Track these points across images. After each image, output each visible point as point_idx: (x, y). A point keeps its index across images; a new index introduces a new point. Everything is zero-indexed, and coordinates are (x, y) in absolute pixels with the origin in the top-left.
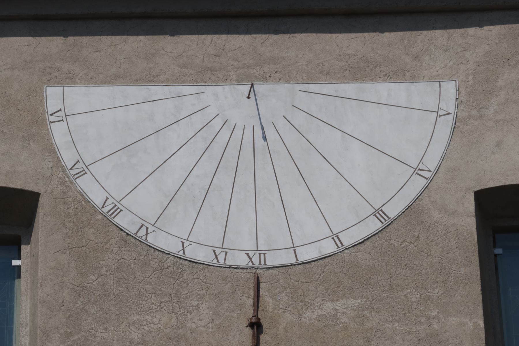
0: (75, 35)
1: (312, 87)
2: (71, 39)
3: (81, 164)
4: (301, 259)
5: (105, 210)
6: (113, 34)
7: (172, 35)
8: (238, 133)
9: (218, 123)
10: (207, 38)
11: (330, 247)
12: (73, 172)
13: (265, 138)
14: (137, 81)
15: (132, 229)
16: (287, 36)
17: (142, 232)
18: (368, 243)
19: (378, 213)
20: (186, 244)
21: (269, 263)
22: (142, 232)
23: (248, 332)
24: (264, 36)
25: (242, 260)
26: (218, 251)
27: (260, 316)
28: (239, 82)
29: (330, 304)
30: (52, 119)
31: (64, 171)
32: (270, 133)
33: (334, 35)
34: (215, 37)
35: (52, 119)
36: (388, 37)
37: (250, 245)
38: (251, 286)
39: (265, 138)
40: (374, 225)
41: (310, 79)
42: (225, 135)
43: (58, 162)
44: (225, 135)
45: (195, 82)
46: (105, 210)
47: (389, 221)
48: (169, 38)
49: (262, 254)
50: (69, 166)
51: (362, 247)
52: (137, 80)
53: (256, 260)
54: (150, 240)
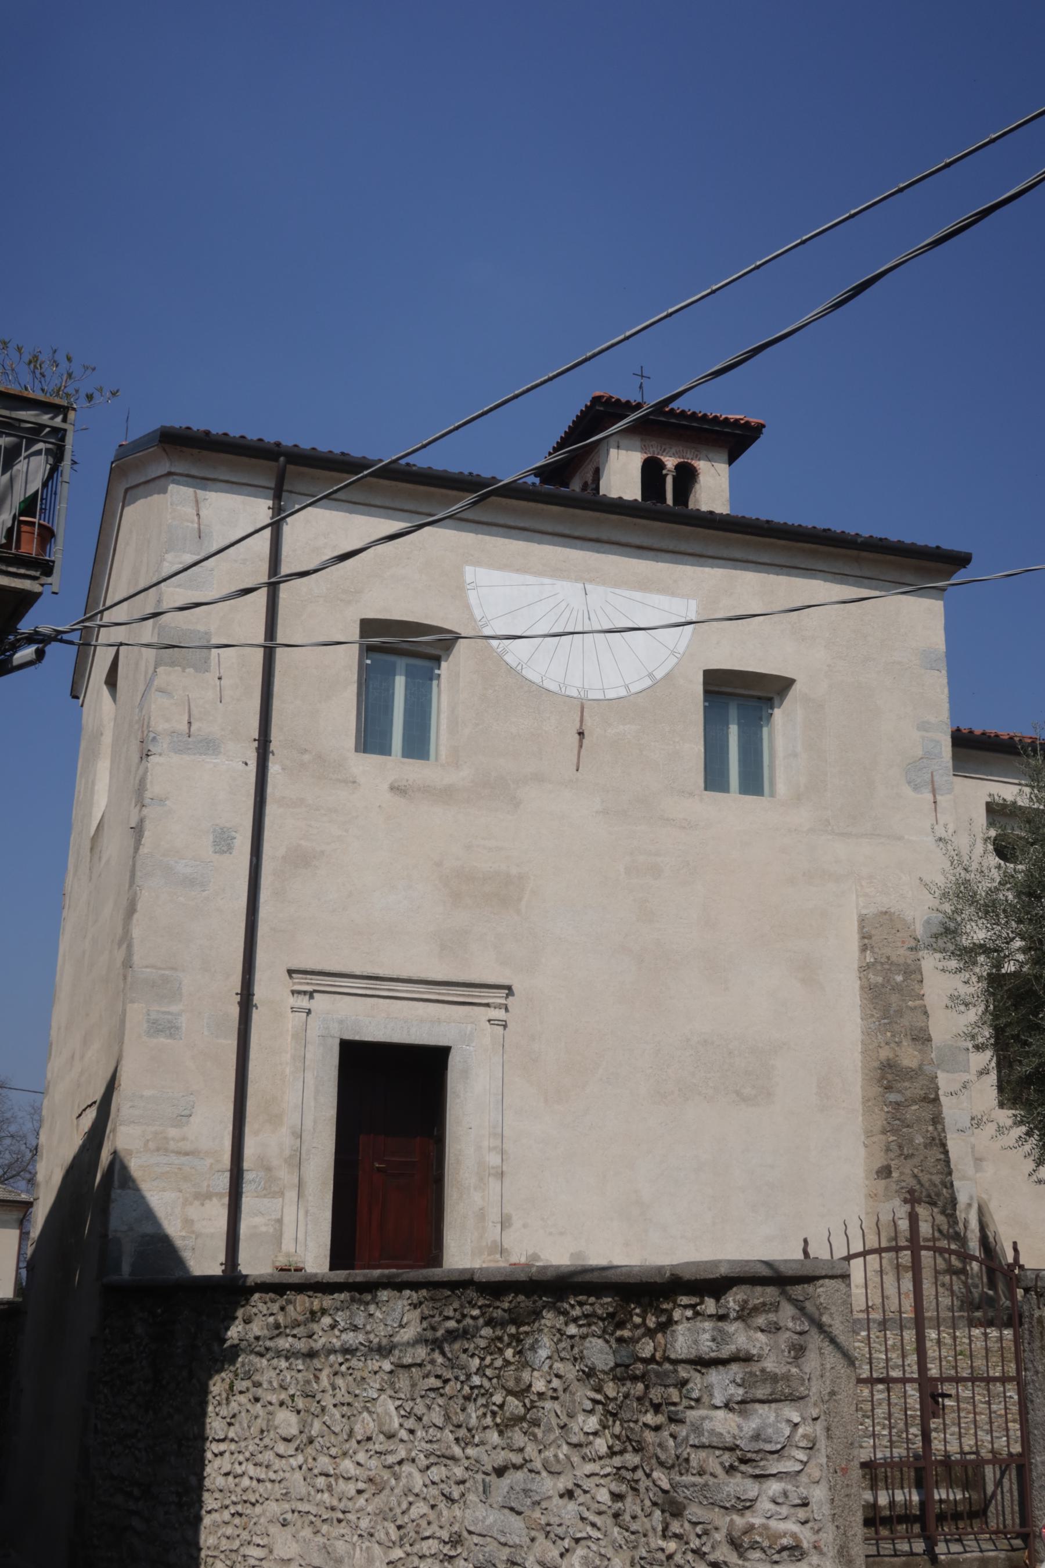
0: (482, 534)
1: (617, 591)
2: (480, 536)
3: (484, 619)
4: (608, 697)
5: (499, 650)
6: (504, 537)
7: (539, 543)
8: (575, 613)
9: (563, 605)
10: (559, 549)
11: (623, 692)
12: (481, 623)
13: (589, 619)
14: (518, 571)
15: (514, 665)
16: (604, 555)
17: (519, 668)
18: (644, 693)
19: (650, 675)
20: (544, 678)
21: (590, 697)
22: (519, 668)
23: (577, 737)
24: (591, 553)
25: (575, 694)
26: (562, 685)
27: (584, 728)
28: (576, 580)
29: (621, 727)
30: (469, 587)
31: (475, 621)
32: (593, 616)
33: (631, 559)
34: (564, 549)
35: (469, 587)
36: (661, 565)
37: (579, 684)
38: (579, 709)
39: (589, 619)
40: (648, 682)
41: (616, 585)
42: (567, 614)
43: (472, 615)
44: (567, 614)
45: (552, 576)
46: (499, 650)
47: (656, 681)
48: (536, 545)
49: (586, 692)
50: (479, 619)
51: (640, 695)
52: (518, 570)
53: (582, 693)
54: (524, 673)
